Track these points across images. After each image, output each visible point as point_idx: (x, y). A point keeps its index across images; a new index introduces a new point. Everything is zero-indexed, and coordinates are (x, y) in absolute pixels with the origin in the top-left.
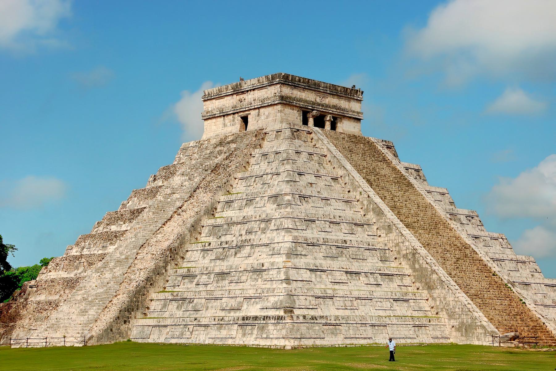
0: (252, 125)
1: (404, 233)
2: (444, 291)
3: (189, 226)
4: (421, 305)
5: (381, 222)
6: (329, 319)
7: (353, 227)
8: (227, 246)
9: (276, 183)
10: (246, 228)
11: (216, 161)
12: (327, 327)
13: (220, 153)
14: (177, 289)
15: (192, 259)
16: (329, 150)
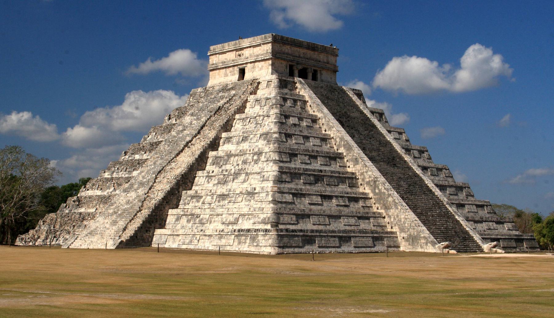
0: (248, 76)
1: (368, 164)
2: (397, 211)
3: (197, 157)
4: (379, 221)
8: (227, 173)
9: (267, 123)
10: (242, 159)
11: (219, 104)
13: (222, 98)
14: (187, 207)
15: (199, 183)
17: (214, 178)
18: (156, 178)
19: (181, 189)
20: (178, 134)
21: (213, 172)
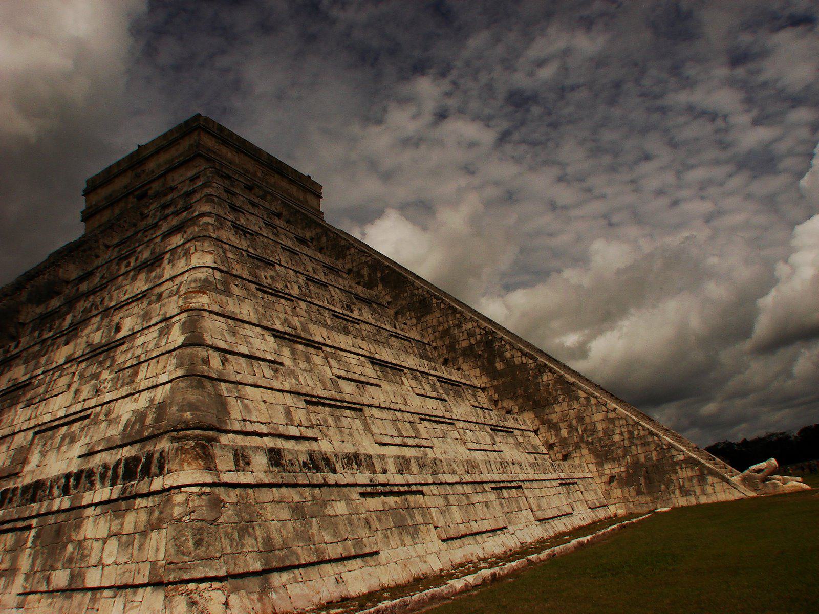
2: (577, 406)
5: (404, 298)
6: (378, 467)
7: (354, 300)
8: (51, 334)
12: (374, 503)
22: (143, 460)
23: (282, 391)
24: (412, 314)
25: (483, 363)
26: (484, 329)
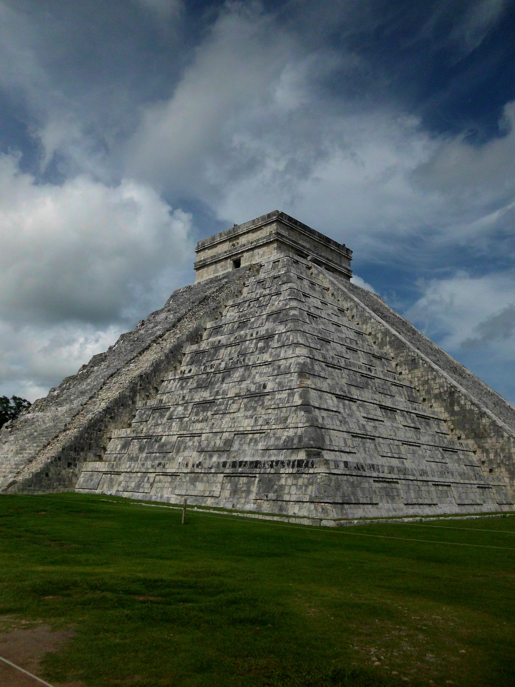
2: (501, 441)
3: (167, 351)
7: (372, 358)
8: (213, 370)
15: (168, 390)
16: (332, 283)
17: (191, 380)
18: (104, 384)
19: (138, 397)
20: (146, 331)
21: (190, 371)
22: (305, 462)
23: (343, 432)
24: (406, 367)
25: (446, 405)
26: (450, 384)
